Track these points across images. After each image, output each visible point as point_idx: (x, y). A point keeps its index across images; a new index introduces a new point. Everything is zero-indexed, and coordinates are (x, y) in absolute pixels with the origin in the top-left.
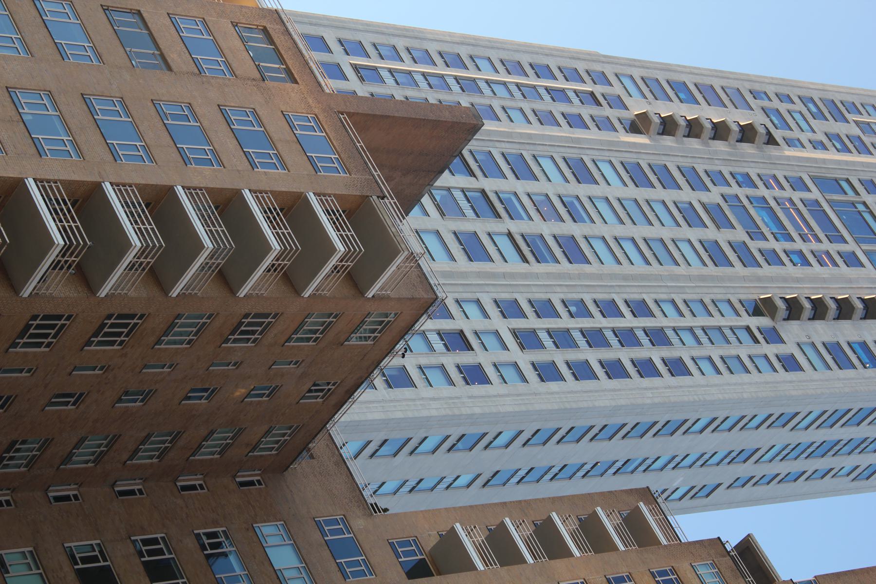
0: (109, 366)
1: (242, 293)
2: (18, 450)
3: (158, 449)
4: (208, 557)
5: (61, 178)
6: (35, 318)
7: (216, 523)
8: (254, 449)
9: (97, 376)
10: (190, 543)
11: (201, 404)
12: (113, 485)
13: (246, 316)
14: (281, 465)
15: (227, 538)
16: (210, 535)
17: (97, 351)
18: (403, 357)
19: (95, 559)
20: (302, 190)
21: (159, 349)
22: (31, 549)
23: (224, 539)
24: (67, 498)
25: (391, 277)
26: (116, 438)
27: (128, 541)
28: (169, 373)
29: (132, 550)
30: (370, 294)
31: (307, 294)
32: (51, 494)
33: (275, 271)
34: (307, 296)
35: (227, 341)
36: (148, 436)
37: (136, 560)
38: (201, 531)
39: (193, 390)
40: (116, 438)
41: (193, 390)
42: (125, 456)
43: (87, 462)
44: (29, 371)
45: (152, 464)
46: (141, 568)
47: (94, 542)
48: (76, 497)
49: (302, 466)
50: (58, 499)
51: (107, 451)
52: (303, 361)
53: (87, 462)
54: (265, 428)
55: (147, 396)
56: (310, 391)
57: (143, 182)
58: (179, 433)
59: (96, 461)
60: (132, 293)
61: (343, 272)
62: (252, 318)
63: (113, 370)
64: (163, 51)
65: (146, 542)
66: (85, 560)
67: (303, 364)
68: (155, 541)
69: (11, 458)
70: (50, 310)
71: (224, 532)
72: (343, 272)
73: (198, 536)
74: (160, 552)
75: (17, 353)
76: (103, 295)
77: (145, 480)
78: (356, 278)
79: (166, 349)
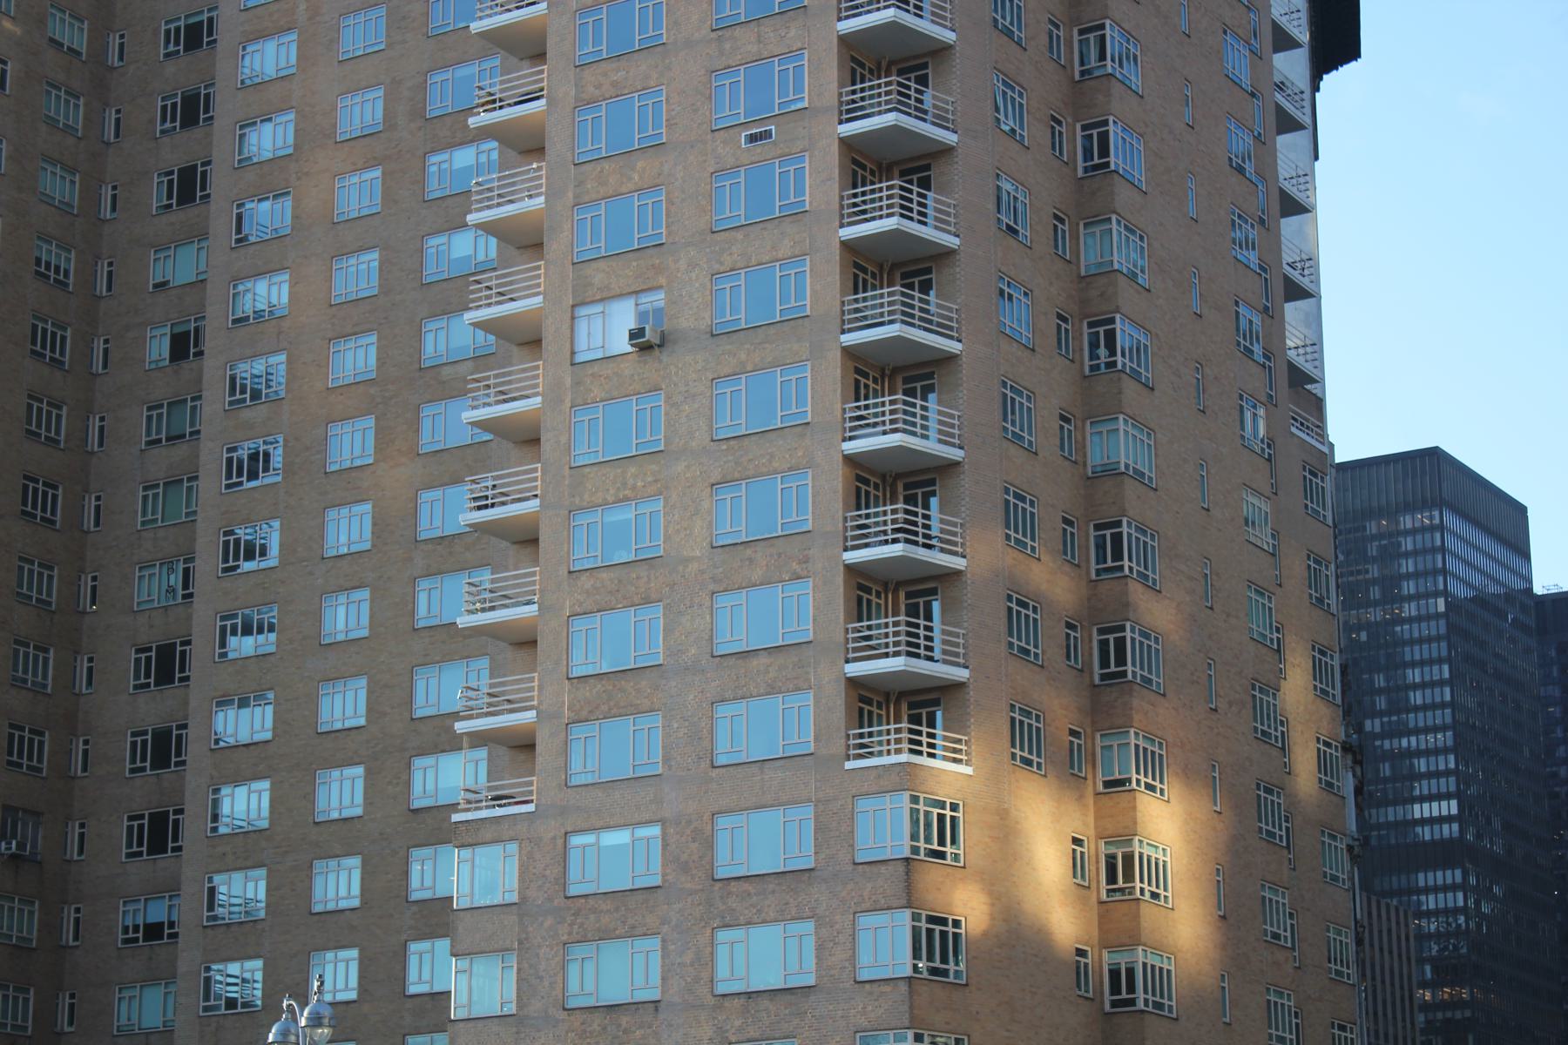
2: (48, 265)
3: (67, 102)
7: (156, 32)
10: (171, 68)
12: (108, 144)
16: (167, 42)
19: (171, 182)
24: (114, 197)
29: (166, 140)
38: (162, 52)
43: (73, 182)
45: (86, 105)
48: (114, 188)
50: (114, 209)
53: (73, 182)
59: (72, 171)
65: (164, 120)
66: (170, 197)
68: (164, 108)
69: (57, 269)
74: (174, 105)
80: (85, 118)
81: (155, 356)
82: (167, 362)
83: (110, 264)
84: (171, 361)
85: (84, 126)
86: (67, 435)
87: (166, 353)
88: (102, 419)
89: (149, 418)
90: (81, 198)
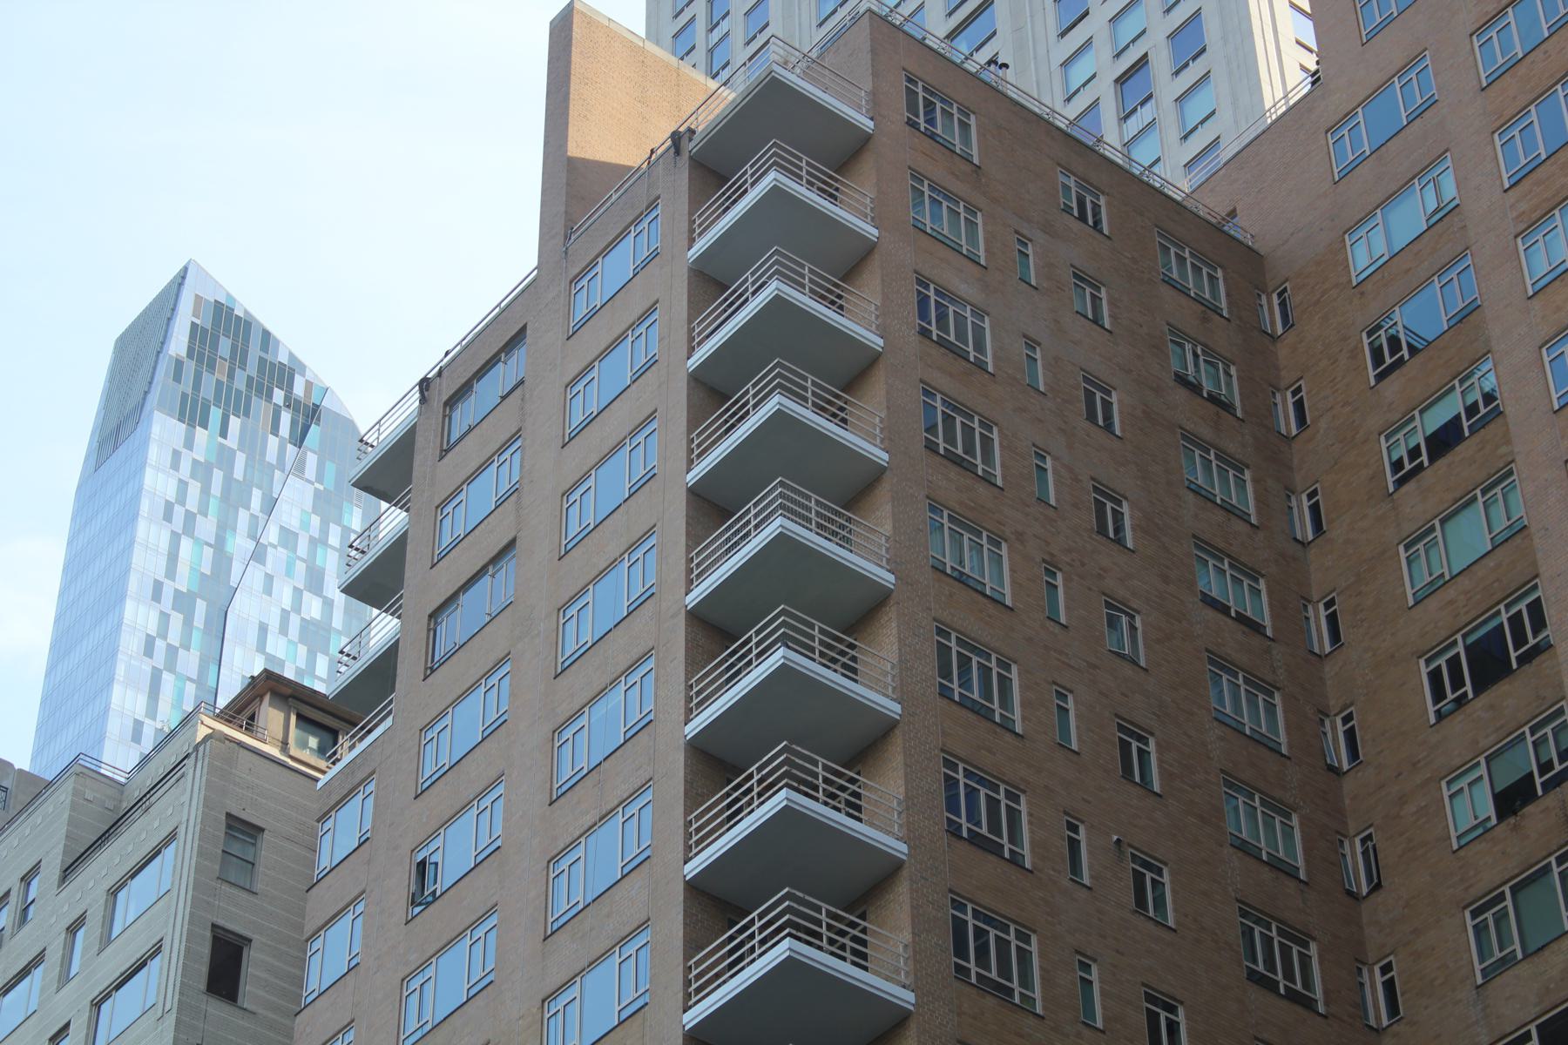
0: (1044, 561)
1: (876, 342)
4: (1413, 350)
5: (683, 678)
6: (945, 693)
7: (1356, 352)
8: (1217, 311)
9: (1066, 580)
11: (1120, 401)
12: (1304, 544)
13: (924, 333)
14: (1246, 265)
15: (1379, 327)
17: (1014, 582)
18: (1005, 66)
20: (685, 270)
21: (1004, 478)
22: (1422, 662)
23: (1382, 332)
24: (1332, 619)
25: (839, 96)
26: (1202, 544)
27: (1395, 496)
28: (1055, 459)
30: (868, 124)
31: (872, 232)
32: (1328, 649)
33: (840, 297)
34: (875, 232)
35: (980, 365)
36: (1197, 491)
37: (1427, 476)
39: (1092, 416)
40: (1202, 544)
41: (1092, 416)
42: (1240, 526)
44: (1063, 697)
45: (1255, 481)
46: (1441, 463)
47: (1403, 555)
48: (1328, 605)
49: (1246, 228)
51: (1229, 556)
52: (1017, 232)
54: (1165, 290)
55: (1105, 494)
56: (1082, 218)
57: (683, 539)
58: (1184, 437)
59: (1254, 576)
60: (887, 528)
61: (836, 180)
62: (929, 323)
63: (1052, 555)
64: (486, 560)
67: (1025, 232)
70: (930, 667)
71: (1369, 334)
72: (836, 180)
73: (1380, 377)
75: (1024, 718)
76: (891, 578)
77: (1290, 491)
78: (840, 154)
79: (1002, 465)
80: (1257, 499)
81: (1466, 822)
82: (1494, 821)
83: (1347, 719)
84: (1501, 816)
85: (1259, 511)
86: (1326, 992)
87: (1488, 809)
88: (1386, 969)
89: (1480, 930)
90: (1274, 616)
